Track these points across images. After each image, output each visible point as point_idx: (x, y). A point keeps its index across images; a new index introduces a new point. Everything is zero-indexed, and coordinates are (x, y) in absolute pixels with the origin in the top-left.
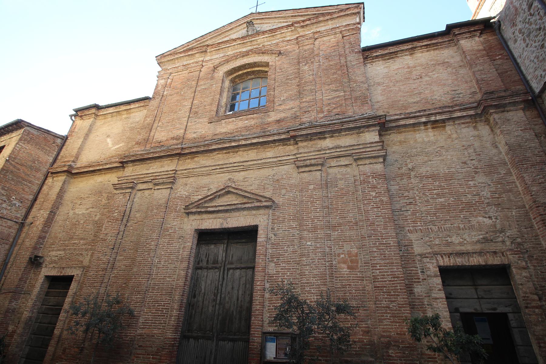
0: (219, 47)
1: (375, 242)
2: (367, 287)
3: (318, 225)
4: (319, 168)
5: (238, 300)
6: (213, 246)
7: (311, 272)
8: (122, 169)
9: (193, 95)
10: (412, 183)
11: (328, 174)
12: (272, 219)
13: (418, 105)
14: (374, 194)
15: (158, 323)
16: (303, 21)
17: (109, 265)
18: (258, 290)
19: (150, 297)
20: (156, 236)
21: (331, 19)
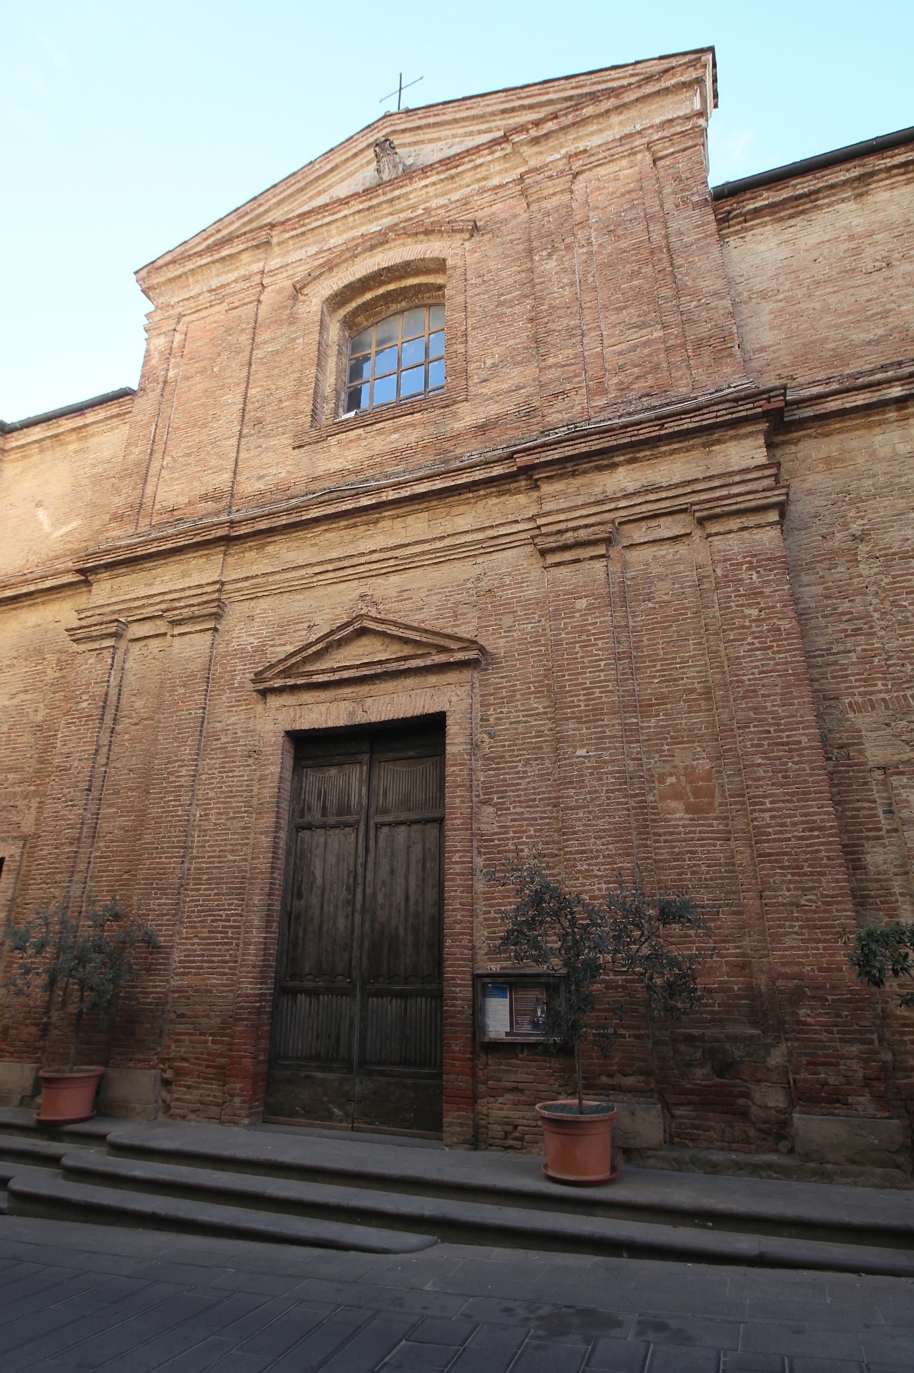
0: (304, 225)
1: (759, 739)
2: (739, 857)
3: (604, 703)
4: (601, 550)
5: (407, 899)
6: (333, 772)
7: (590, 825)
8: (84, 589)
9: (244, 373)
10: (860, 576)
11: (625, 565)
12: (481, 696)
13: (880, 348)
14: (754, 612)
15: (218, 962)
16: (537, 124)
17: (85, 830)
18: (457, 874)
19: (192, 901)
20: (190, 754)
21: (616, 108)
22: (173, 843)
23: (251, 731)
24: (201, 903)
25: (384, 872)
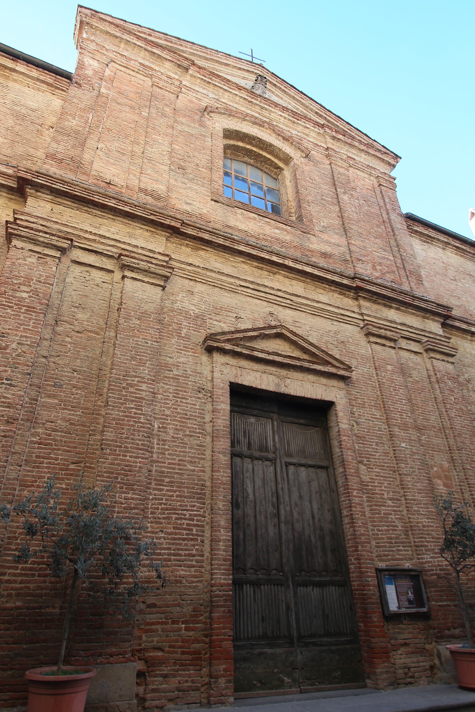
5: (313, 517)
6: (252, 420)
15: (185, 555)
22: (138, 444)
23: (199, 373)
24: (164, 501)
25: (295, 495)
